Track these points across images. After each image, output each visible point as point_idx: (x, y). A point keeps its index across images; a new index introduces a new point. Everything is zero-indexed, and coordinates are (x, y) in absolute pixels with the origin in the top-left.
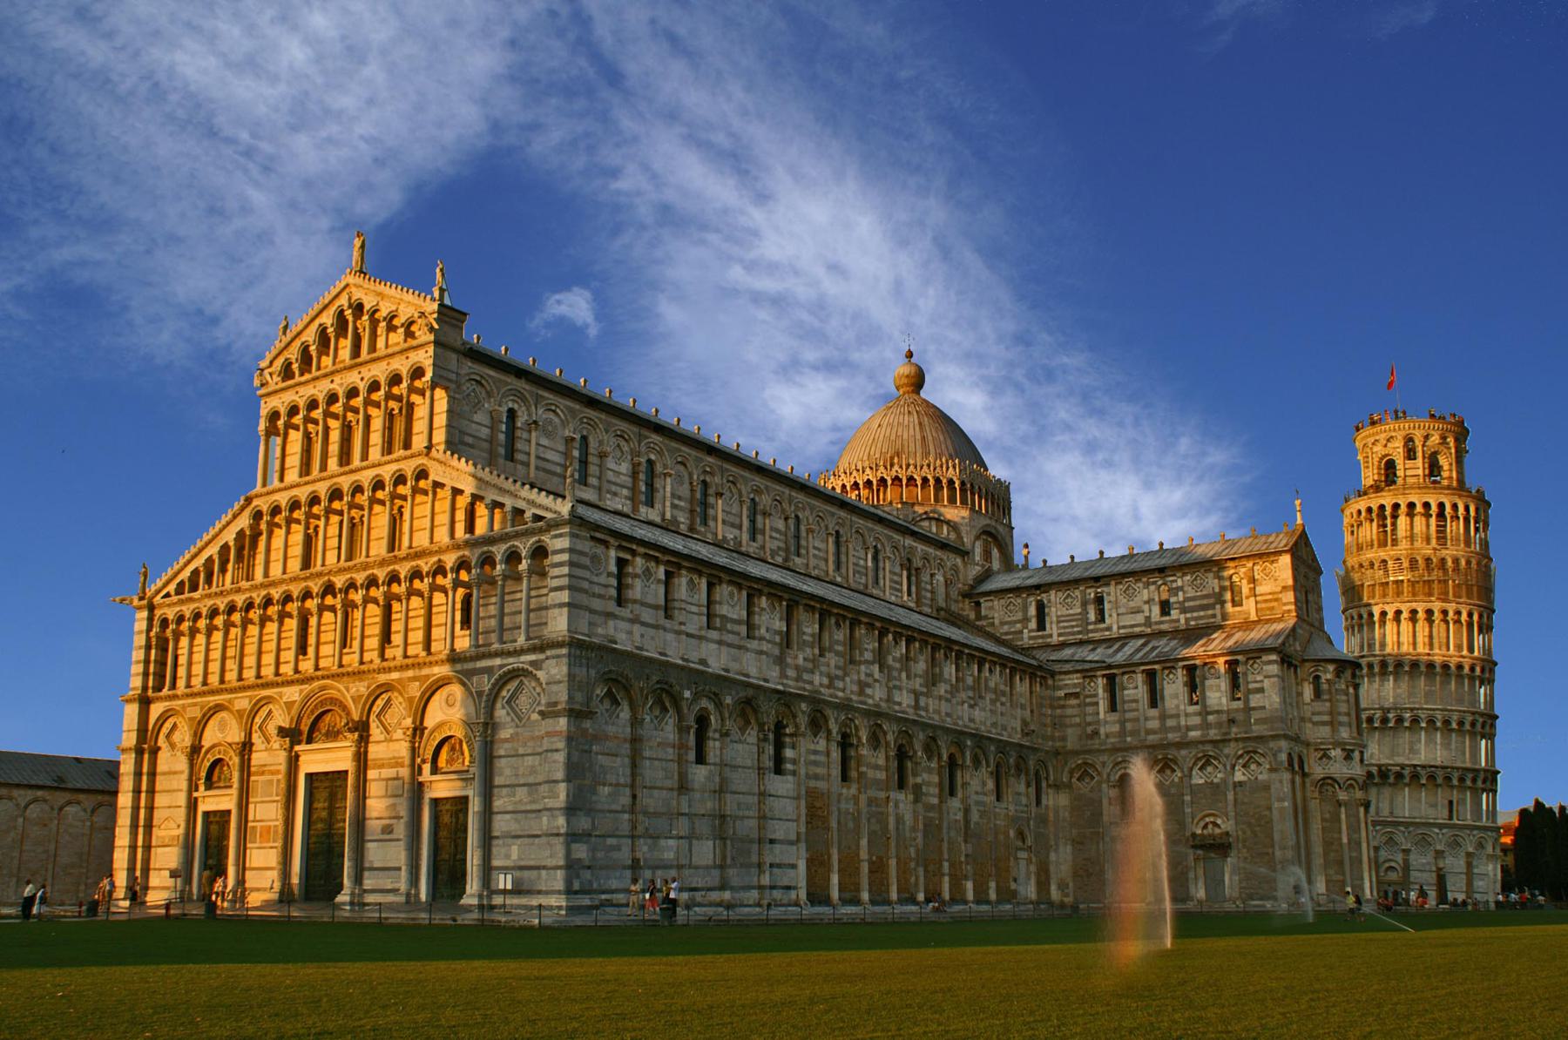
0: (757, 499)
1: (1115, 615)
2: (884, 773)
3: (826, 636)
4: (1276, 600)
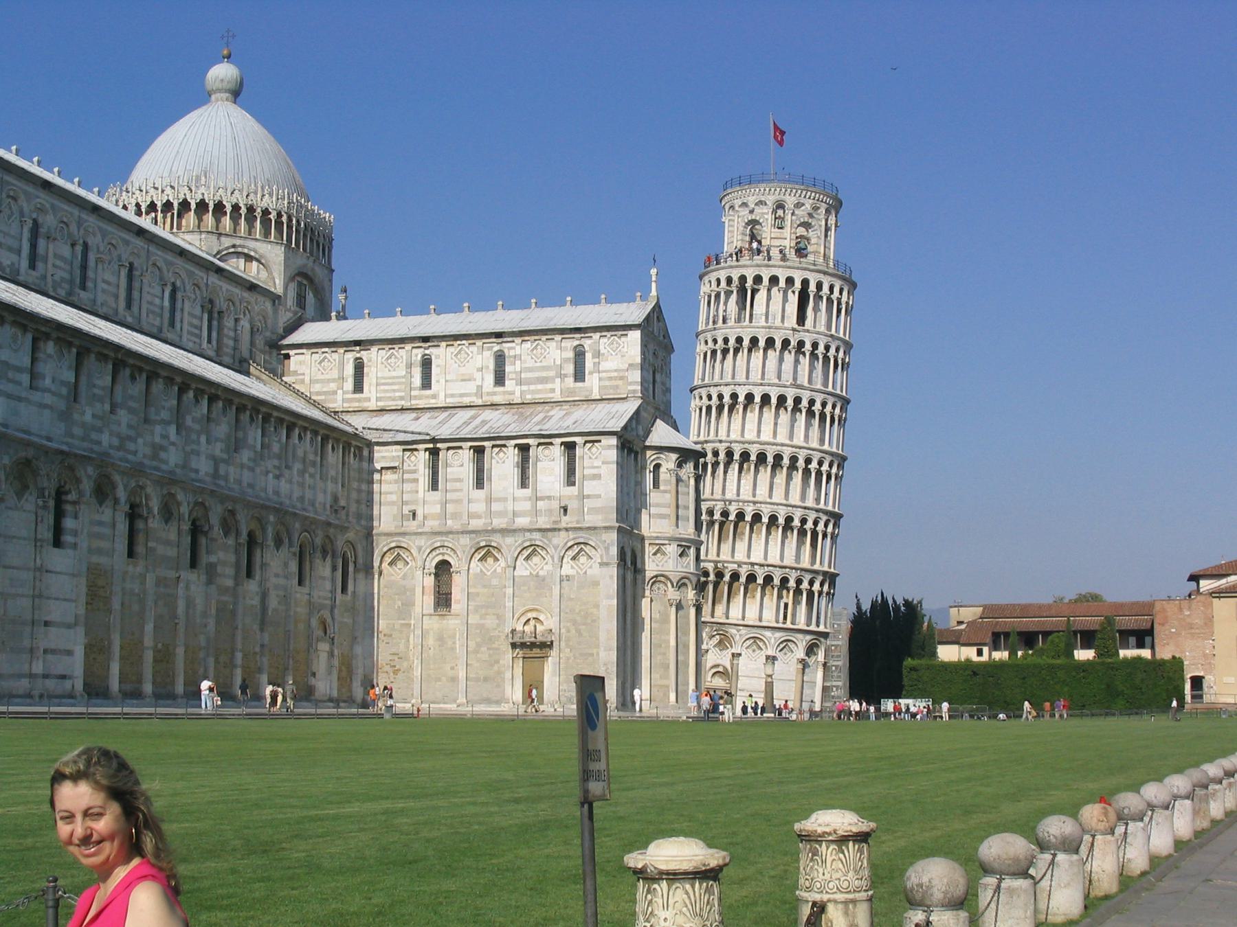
0: (40, 220)
1: (442, 381)
2: (175, 550)
3: (119, 389)
4: (621, 378)
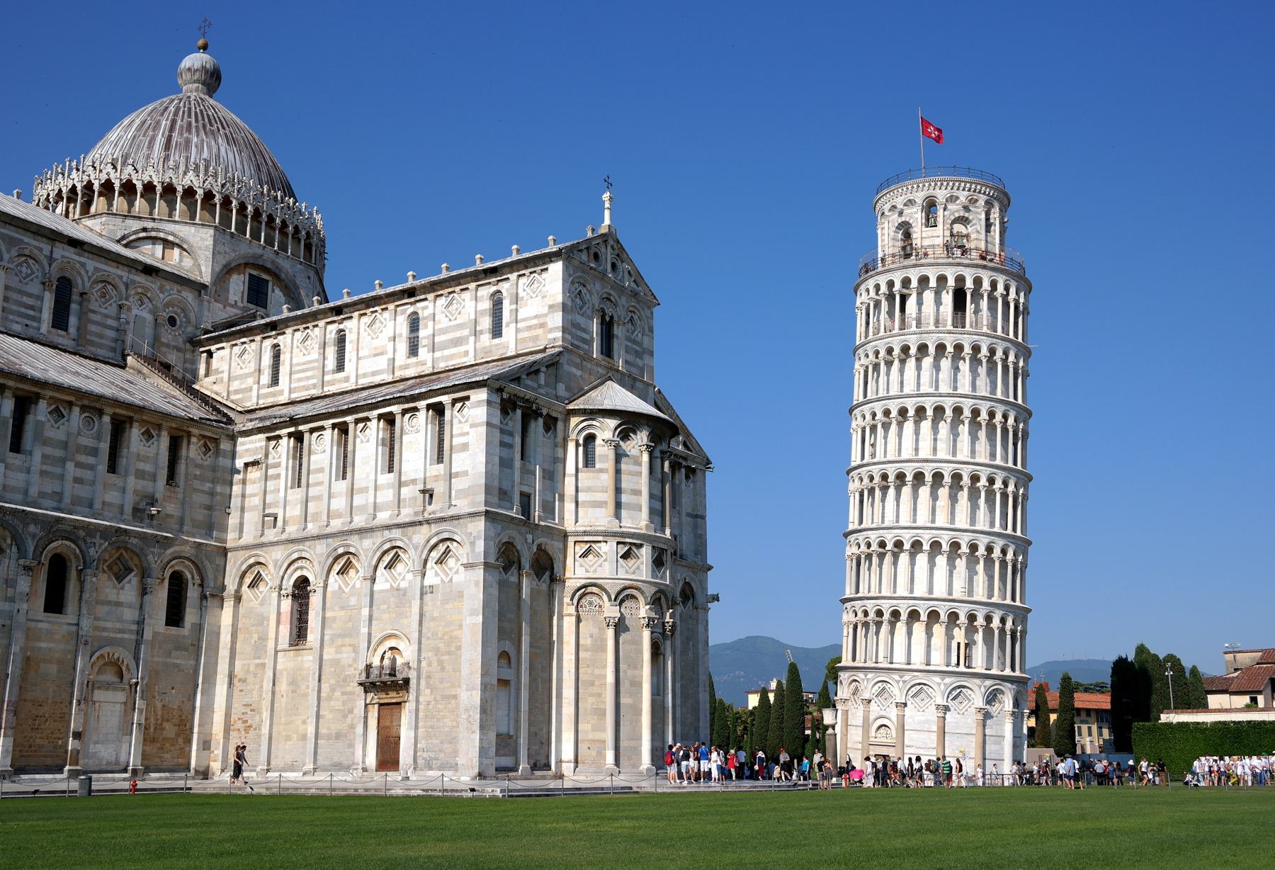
4: (542, 325)
